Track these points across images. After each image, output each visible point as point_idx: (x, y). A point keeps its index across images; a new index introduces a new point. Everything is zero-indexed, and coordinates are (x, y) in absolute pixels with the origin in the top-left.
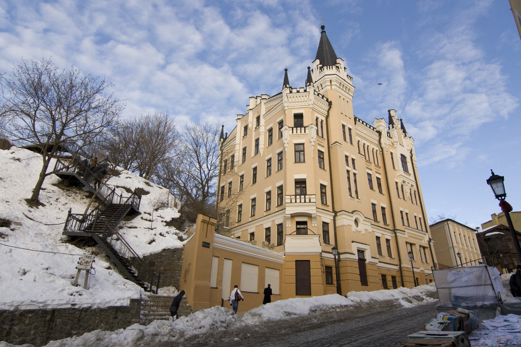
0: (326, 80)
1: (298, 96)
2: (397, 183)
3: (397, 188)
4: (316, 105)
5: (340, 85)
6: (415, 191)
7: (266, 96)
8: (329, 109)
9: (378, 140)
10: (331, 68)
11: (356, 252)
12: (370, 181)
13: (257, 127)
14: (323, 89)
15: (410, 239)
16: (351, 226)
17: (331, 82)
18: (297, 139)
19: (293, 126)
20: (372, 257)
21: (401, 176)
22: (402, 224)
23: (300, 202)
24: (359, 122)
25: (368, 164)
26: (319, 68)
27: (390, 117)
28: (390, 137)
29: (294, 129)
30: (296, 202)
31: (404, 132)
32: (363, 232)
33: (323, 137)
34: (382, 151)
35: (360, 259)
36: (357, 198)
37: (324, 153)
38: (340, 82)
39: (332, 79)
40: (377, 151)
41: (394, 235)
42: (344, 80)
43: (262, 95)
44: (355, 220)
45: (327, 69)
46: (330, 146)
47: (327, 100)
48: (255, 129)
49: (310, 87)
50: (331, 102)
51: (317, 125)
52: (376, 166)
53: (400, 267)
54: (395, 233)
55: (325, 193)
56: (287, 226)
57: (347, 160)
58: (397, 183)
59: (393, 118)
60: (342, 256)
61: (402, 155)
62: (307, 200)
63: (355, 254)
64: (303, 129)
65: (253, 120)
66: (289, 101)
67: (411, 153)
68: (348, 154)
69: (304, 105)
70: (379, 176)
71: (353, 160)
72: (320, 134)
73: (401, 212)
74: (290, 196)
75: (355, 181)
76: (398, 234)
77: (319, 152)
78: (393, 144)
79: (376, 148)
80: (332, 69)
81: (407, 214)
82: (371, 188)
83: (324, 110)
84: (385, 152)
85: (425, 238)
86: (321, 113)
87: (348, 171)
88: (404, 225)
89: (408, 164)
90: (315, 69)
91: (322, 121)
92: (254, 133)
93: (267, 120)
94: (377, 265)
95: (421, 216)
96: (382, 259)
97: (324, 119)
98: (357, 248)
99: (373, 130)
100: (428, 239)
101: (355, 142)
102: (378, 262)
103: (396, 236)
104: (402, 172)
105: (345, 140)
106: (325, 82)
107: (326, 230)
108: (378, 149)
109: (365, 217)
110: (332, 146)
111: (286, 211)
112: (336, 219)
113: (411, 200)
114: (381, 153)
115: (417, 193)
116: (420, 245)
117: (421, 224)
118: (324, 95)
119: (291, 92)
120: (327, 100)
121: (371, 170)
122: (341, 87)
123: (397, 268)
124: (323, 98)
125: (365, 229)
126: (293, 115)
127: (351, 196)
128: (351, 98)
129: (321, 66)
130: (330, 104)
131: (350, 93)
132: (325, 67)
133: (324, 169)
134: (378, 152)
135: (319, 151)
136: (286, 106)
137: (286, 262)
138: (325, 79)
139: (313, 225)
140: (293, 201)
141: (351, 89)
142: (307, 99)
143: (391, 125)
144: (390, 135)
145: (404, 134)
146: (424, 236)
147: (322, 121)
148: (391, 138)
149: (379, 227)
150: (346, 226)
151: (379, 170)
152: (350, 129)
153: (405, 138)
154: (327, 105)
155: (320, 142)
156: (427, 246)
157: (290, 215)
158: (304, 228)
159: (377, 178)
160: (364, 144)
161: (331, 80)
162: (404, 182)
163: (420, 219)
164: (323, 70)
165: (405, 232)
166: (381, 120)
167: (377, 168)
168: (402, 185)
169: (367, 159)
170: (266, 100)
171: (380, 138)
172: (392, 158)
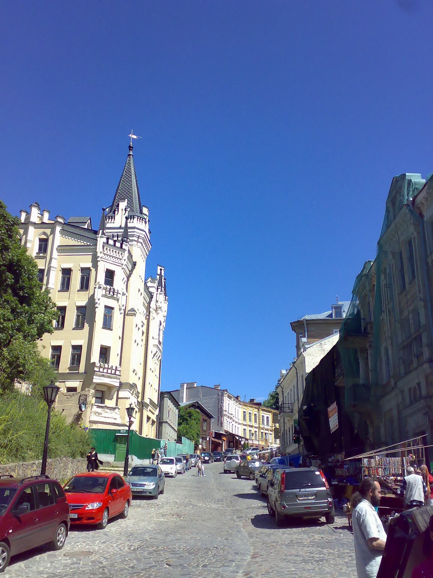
10: (141, 221)
17: (138, 238)
34: (149, 316)
38: (145, 240)
39: (141, 235)
45: (138, 221)
65: (34, 239)
110: (129, 312)
126: (105, 270)
130: (134, 264)
132: (136, 217)
136: (100, 257)
138: (134, 232)
143: (160, 287)
145: (165, 296)
162: (157, 352)
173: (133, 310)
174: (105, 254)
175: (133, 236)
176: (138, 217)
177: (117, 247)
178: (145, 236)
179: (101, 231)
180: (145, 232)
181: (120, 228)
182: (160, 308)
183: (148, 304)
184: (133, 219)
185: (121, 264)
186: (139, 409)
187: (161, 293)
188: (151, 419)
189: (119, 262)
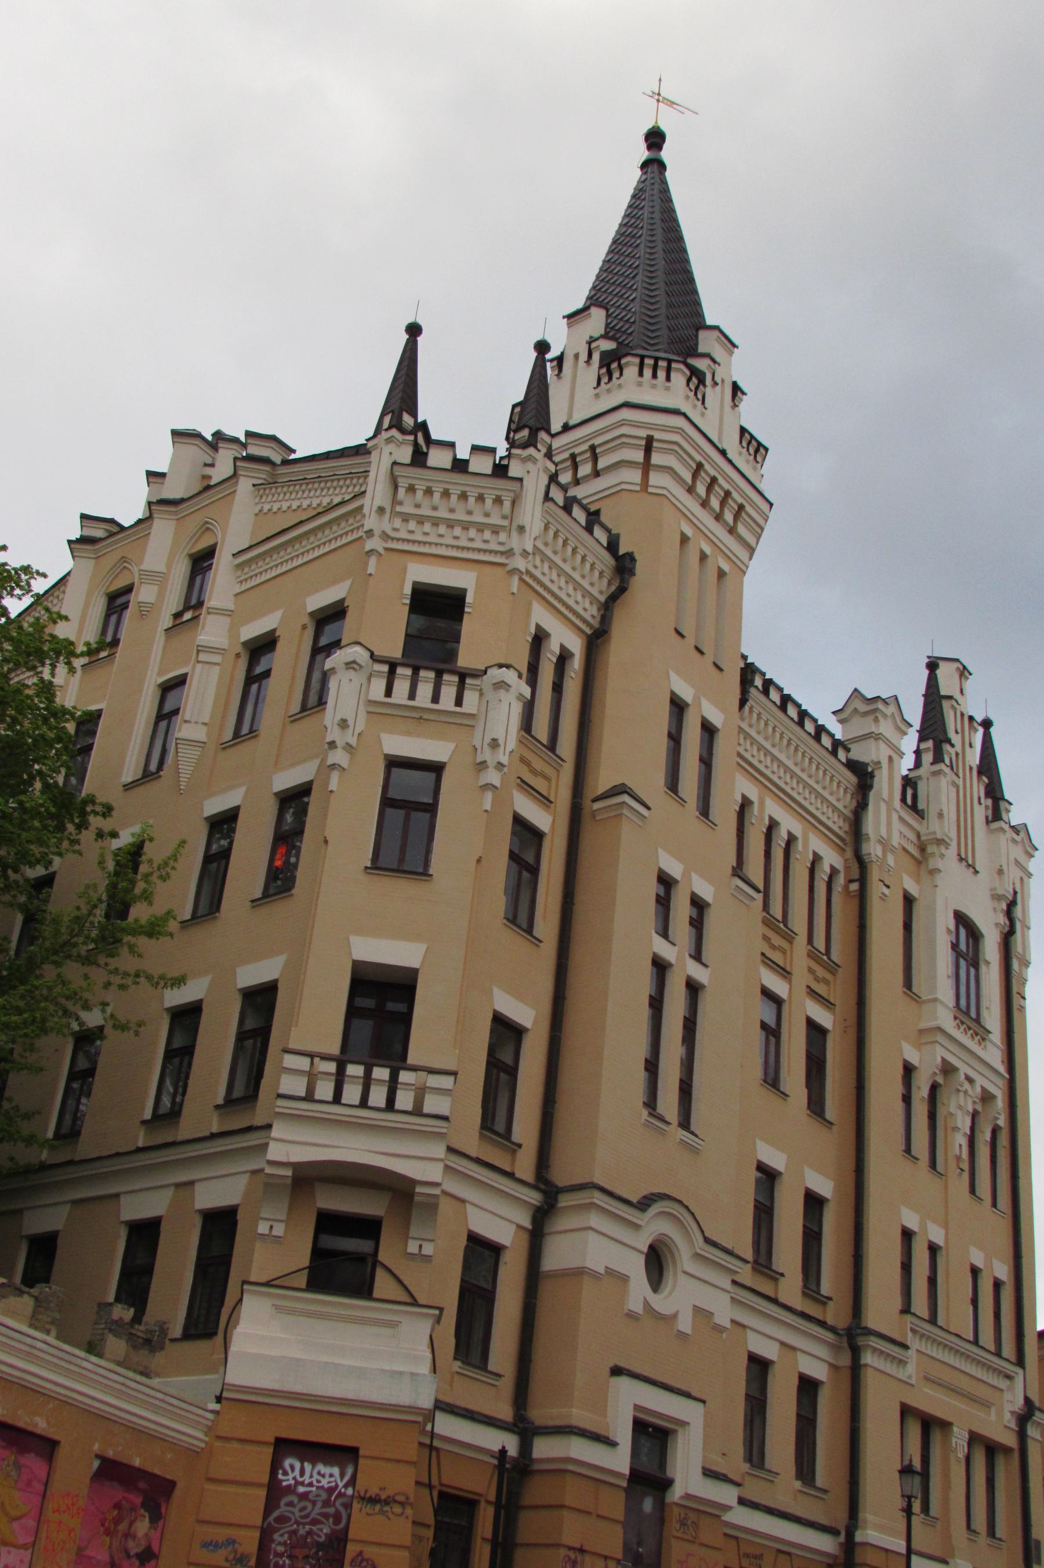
1: (455, 491)
2: (908, 1070)
3: (907, 1099)
4: (544, 558)
5: (695, 475)
6: (995, 1131)
7: (273, 444)
8: (614, 598)
9: (847, 812)
10: (661, 374)
11: (624, 1435)
12: (772, 1032)
13: (188, 616)
14: (596, 474)
15: (929, 1390)
16: (624, 1279)
17: (648, 449)
18: (408, 733)
19: (397, 653)
20: (709, 1473)
21: (940, 1038)
22: (898, 1304)
23: (364, 1103)
24: (762, 698)
25: (777, 940)
26: (596, 357)
27: (933, 699)
28: (914, 808)
29: (400, 670)
30: (337, 1099)
31: (994, 792)
32: (685, 1324)
33: (552, 745)
34: (863, 879)
35: (637, 1477)
36: (685, 1123)
37: (546, 843)
38: (698, 458)
40: (834, 871)
41: (845, 1360)
42: (723, 453)
43: (249, 434)
44: (651, 1247)
45: (641, 374)
46: (587, 803)
47: (612, 546)
48: (167, 621)
49: (530, 458)
50: (630, 557)
51: (533, 669)
52: (813, 955)
53: (850, 1546)
54: (856, 1351)
55: (512, 1071)
56: (263, 1228)
57: (664, 902)
58: (908, 1070)
59: (946, 704)
60: (544, 1448)
61: (961, 919)
62: (404, 1100)
63: (612, 1444)
64: (449, 684)
66: (398, 509)
67: (1009, 913)
68: (674, 869)
69: (478, 544)
70: (824, 1018)
71: (699, 904)
72: (541, 729)
73: (907, 1235)
74: (311, 1056)
75: (690, 1026)
76: (868, 1358)
77: (518, 828)
78: (922, 849)
79: (831, 858)
80: (668, 379)
81: (933, 1249)
82: (772, 1080)
83: (586, 594)
84: (876, 889)
85: (1007, 1396)
86: (568, 607)
87: (660, 967)
88: (906, 1310)
89: (983, 968)
90: (577, 356)
91: (564, 657)
92: (160, 638)
93: (249, 585)
94: (728, 1517)
95: (1002, 1271)
96: (755, 1490)
97: (576, 645)
98: (636, 1407)
99: (834, 753)
100: (1021, 1401)
101: (724, 810)
102: (733, 1502)
103: (856, 1370)
104: (946, 1019)
105: (673, 784)
107: (485, 1286)
108: (839, 864)
109: (707, 1240)
110: (597, 806)
111: (272, 1145)
112: (546, 1231)
113: (966, 1176)
114: (854, 887)
115: (1003, 1140)
117: (997, 1315)
118: (597, 513)
119: (419, 458)
120: (612, 546)
121: (784, 973)
122: (701, 489)
123: (825, 1544)
124: (589, 529)
125: (697, 1309)
126: (408, 590)
127: (651, 1103)
129: (608, 345)
131: (741, 529)
132: (629, 359)
133: (529, 930)
134: (841, 879)
135: (518, 821)
137: (218, 1444)
139: (412, 1247)
140: (325, 1090)
141: (748, 508)
142: (504, 517)
143: (930, 744)
144: (915, 797)
145: (989, 802)
146: (1003, 1384)
147: (564, 657)
148: (920, 814)
149: (774, 1301)
150: (595, 1275)
151: (826, 982)
152: (708, 730)
153: (995, 825)
154: (608, 574)
155: (534, 772)
156: (1009, 1440)
157: (289, 1172)
158: (360, 1258)
159: (811, 1024)
160: (773, 826)
161: (650, 440)
163: (997, 1285)
164: (616, 375)
166: (880, 705)
167: (821, 972)
168: (934, 1088)
169: (777, 911)
170: (267, 468)
171: (861, 807)
172: (908, 927)
174: (406, 518)
175: (620, 442)
176: (642, 358)
178: (680, 431)
180: (685, 415)
182: (940, 842)
183: (846, 818)
184: (621, 374)
185: (502, 553)
186: (834, 1368)
187: (936, 767)
188: (959, 1439)
189: (493, 546)
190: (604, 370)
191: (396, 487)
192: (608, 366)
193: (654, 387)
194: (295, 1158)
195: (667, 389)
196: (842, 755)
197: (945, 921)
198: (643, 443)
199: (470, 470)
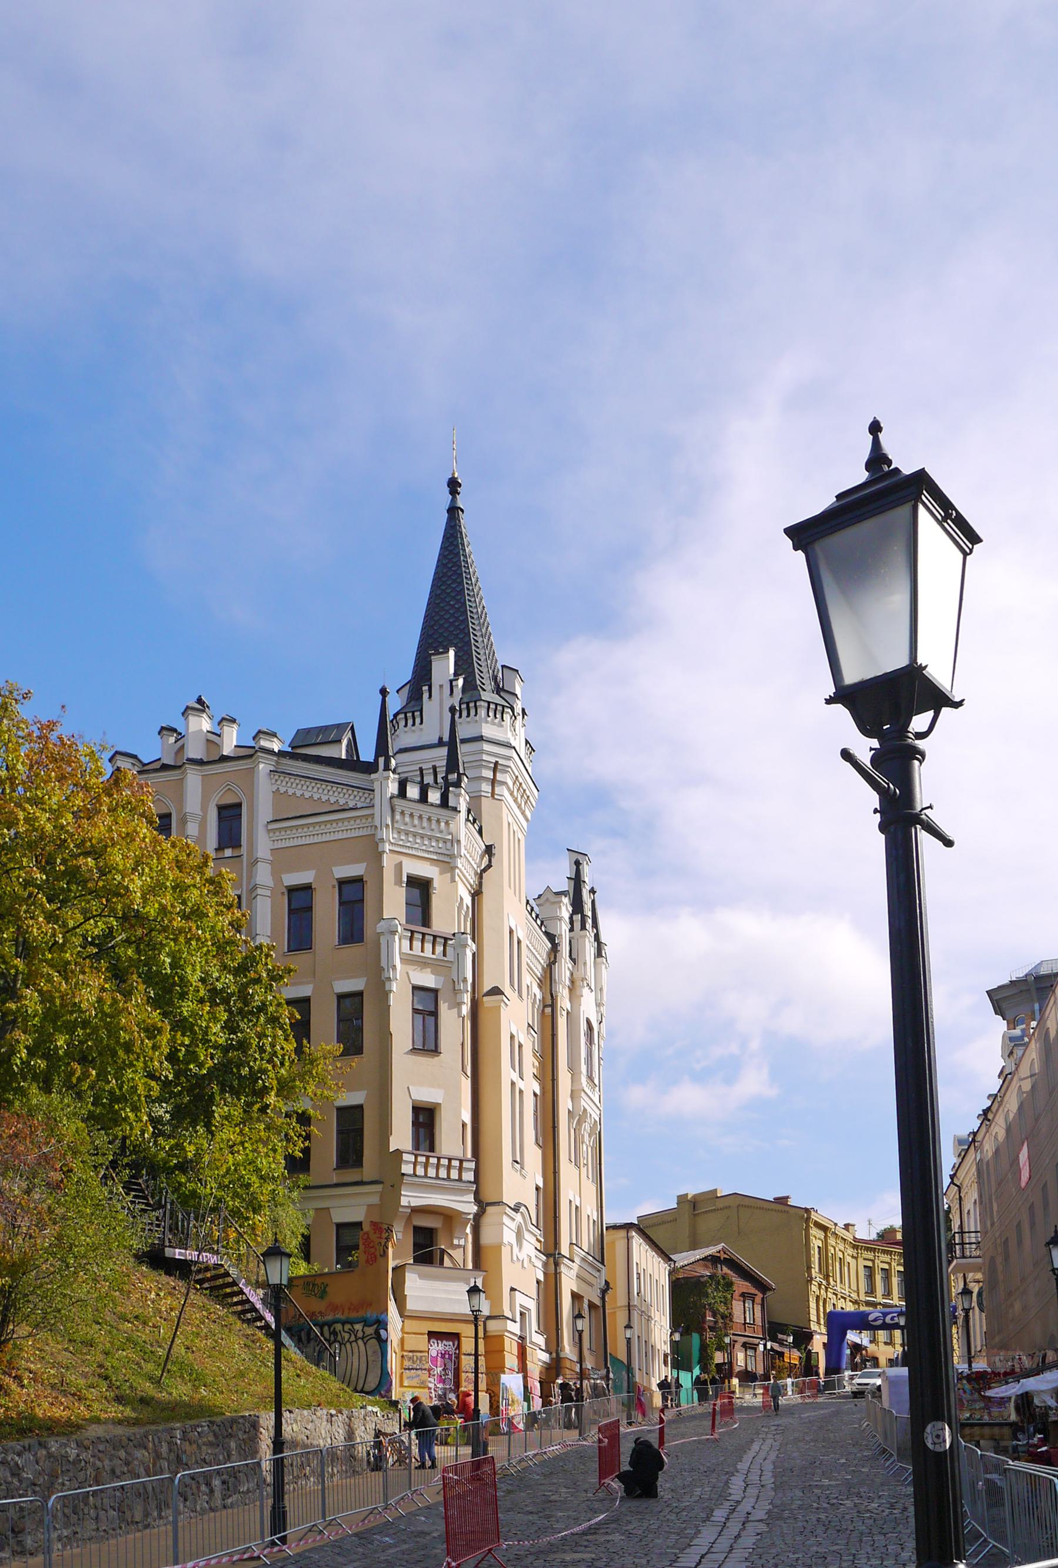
0: (485, 757)
17: (495, 770)
27: (577, 880)
38: (517, 774)
39: (501, 761)
54: (557, 1265)
106: (480, 764)
110: (485, 999)
114: (548, 1010)
116: (589, 1301)
126: (405, 879)
128: (525, 824)
130: (489, 850)
132: (482, 703)
139: (456, 1242)
140: (420, 1171)
156: (597, 1302)
161: (496, 763)
165: (573, 1261)
173: (496, 991)
177: (432, 805)
179: (381, 760)
181: (441, 743)
190: (464, 706)
191: (393, 811)
192: (468, 704)
193: (494, 724)
194: (412, 1205)
195: (502, 726)
196: (543, 929)
197: (583, 1026)
198: (492, 765)
199: (429, 800)
